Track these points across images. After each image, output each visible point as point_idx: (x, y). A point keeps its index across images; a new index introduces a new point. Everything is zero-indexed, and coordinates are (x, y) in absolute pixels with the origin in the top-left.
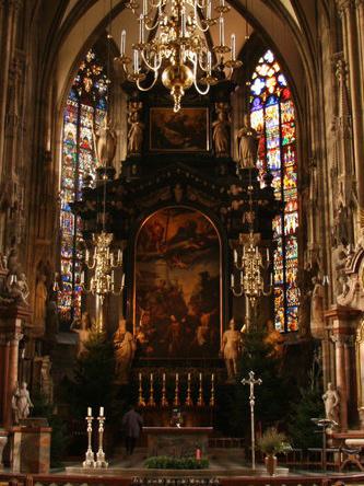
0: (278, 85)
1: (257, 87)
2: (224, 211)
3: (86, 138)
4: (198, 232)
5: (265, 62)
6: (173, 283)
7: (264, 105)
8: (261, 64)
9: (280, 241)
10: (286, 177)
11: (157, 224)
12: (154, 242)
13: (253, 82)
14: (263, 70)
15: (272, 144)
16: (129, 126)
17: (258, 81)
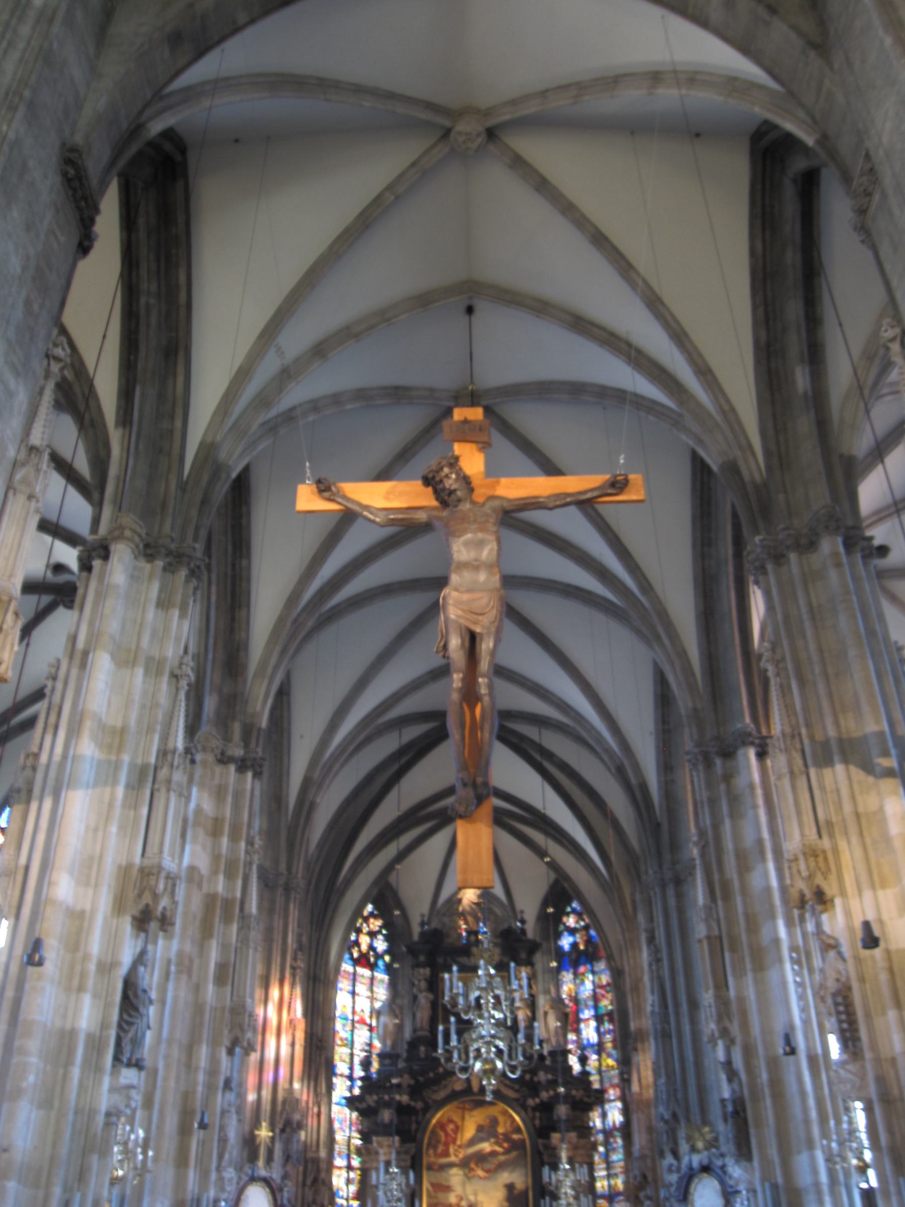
0: (589, 941)
1: (566, 942)
2: (531, 1102)
3: (363, 1011)
4: (501, 1130)
5: (574, 911)
6: (472, 1198)
7: (575, 965)
8: (568, 914)
9: (600, 1137)
10: (604, 1056)
11: (451, 1121)
12: (447, 1145)
13: (558, 935)
14: (571, 921)
15: (587, 1014)
16: (415, 998)
17: (566, 933)
